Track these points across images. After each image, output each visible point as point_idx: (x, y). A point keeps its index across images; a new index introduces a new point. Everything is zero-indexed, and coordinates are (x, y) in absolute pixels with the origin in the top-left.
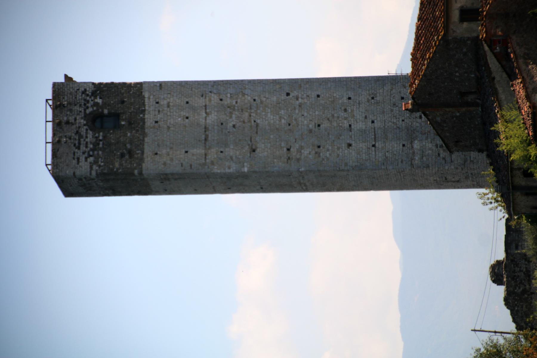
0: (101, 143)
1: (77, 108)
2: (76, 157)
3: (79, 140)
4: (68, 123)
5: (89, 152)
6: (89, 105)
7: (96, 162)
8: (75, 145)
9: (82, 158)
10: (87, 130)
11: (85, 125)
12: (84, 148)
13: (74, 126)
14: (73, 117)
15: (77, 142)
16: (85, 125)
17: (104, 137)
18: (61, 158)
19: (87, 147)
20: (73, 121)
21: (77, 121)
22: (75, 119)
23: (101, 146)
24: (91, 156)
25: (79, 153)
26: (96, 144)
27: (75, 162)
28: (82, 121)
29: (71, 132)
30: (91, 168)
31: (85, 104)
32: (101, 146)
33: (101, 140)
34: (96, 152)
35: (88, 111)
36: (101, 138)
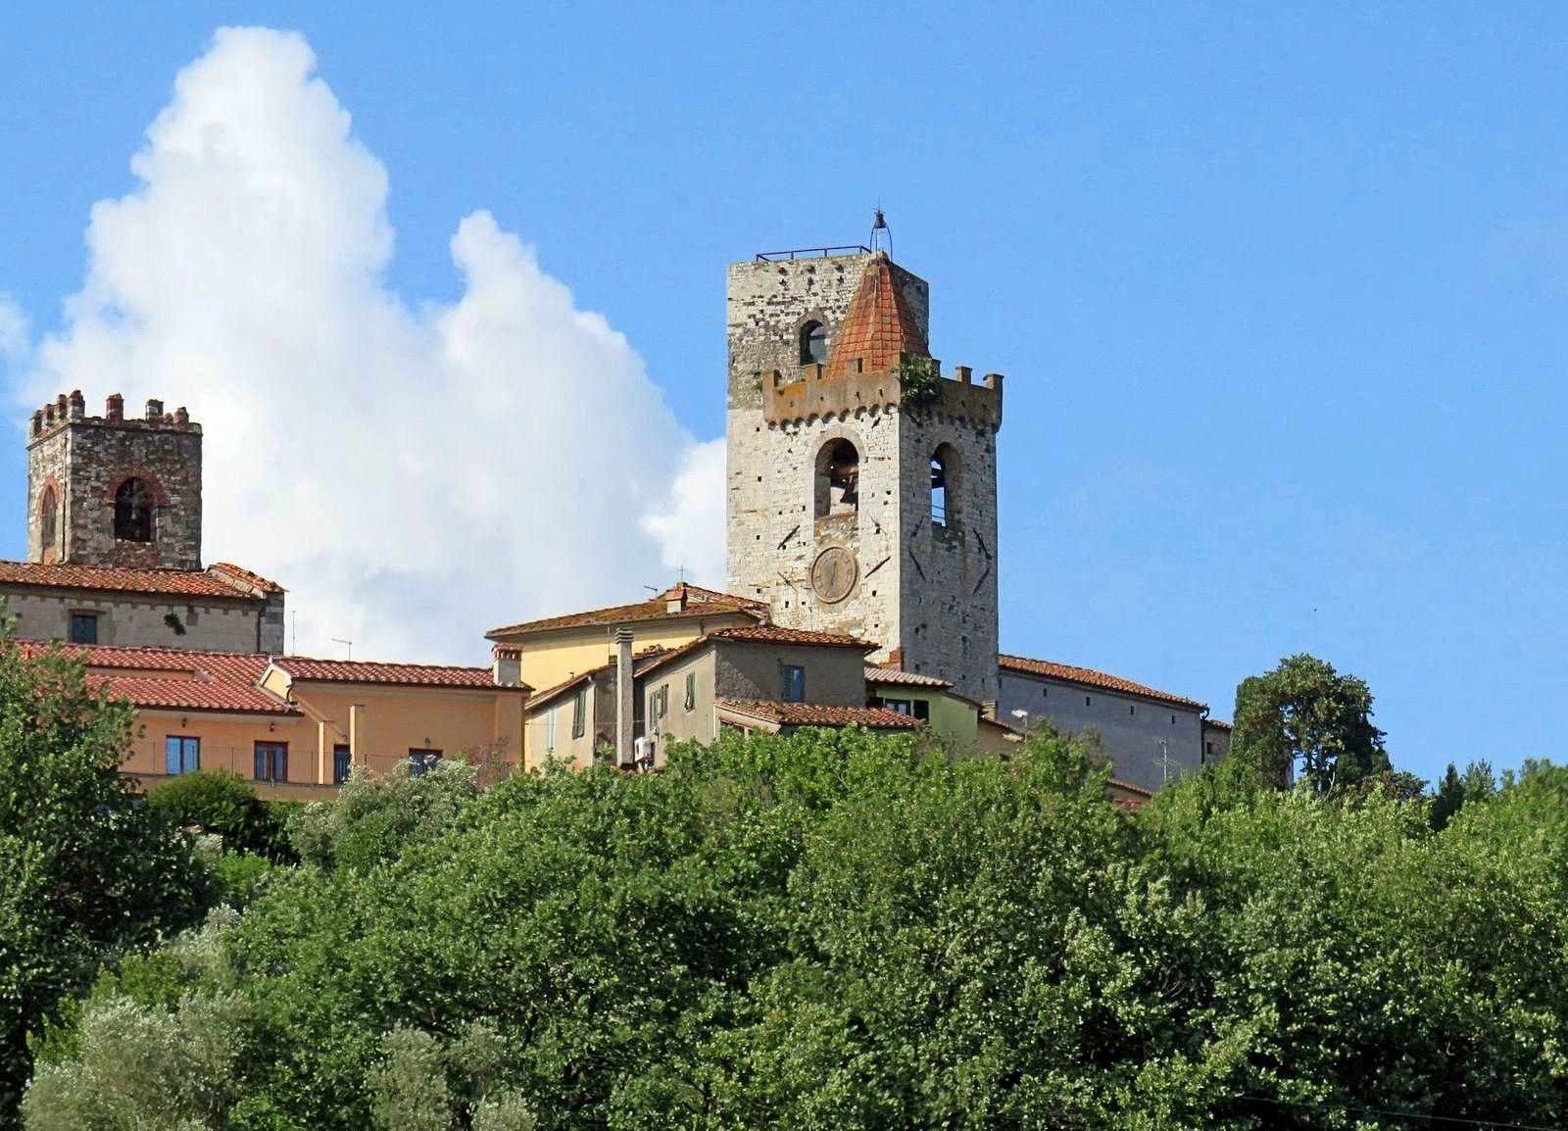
0: (778, 338)
1: (834, 295)
2: (755, 299)
3: (783, 303)
4: (811, 282)
5: (763, 320)
6: (838, 314)
7: (747, 331)
8: (775, 296)
9: (752, 310)
10: (799, 314)
11: (806, 310)
12: (769, 312)
13: (804, 293)
14: (819, 291)
15: (780, 299)
16: (806, 310)
17: (787, 343)
18: (754, 276)
19: (771, 315)
20: (813, 291)
21: (813, 298)
22: (815, 295)
23: (773, 338)
24: (757, 324)
25: (761, 304)
26: (775, 329)
27: (749, 299)
28: (813, 305)
29: (797, 285)
30: (737, 326)
31: (839, 307)
32: (773, 338)
33: (781, 337)
34: (762, 331)
35: (828, 313)
36: (785, 337)
